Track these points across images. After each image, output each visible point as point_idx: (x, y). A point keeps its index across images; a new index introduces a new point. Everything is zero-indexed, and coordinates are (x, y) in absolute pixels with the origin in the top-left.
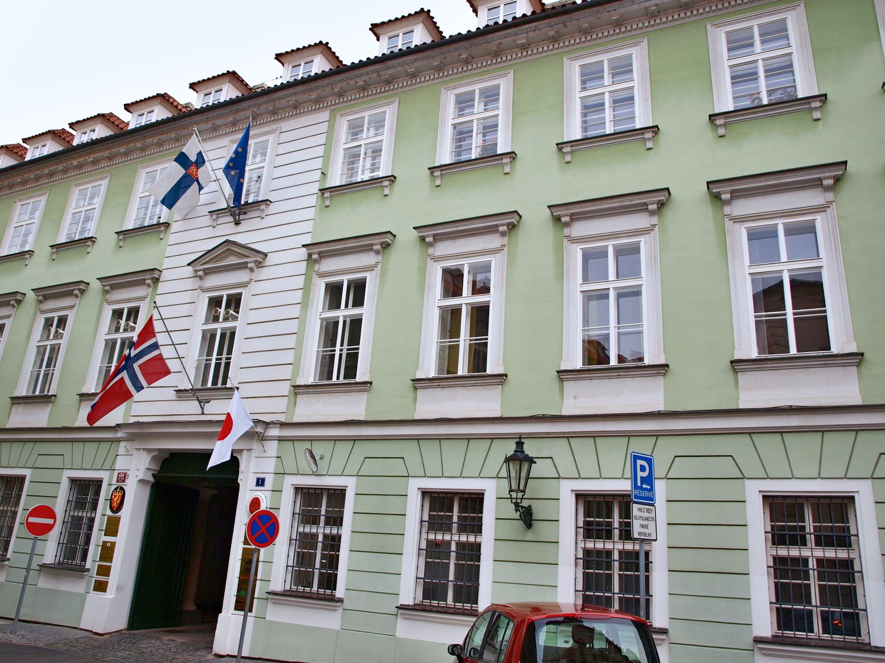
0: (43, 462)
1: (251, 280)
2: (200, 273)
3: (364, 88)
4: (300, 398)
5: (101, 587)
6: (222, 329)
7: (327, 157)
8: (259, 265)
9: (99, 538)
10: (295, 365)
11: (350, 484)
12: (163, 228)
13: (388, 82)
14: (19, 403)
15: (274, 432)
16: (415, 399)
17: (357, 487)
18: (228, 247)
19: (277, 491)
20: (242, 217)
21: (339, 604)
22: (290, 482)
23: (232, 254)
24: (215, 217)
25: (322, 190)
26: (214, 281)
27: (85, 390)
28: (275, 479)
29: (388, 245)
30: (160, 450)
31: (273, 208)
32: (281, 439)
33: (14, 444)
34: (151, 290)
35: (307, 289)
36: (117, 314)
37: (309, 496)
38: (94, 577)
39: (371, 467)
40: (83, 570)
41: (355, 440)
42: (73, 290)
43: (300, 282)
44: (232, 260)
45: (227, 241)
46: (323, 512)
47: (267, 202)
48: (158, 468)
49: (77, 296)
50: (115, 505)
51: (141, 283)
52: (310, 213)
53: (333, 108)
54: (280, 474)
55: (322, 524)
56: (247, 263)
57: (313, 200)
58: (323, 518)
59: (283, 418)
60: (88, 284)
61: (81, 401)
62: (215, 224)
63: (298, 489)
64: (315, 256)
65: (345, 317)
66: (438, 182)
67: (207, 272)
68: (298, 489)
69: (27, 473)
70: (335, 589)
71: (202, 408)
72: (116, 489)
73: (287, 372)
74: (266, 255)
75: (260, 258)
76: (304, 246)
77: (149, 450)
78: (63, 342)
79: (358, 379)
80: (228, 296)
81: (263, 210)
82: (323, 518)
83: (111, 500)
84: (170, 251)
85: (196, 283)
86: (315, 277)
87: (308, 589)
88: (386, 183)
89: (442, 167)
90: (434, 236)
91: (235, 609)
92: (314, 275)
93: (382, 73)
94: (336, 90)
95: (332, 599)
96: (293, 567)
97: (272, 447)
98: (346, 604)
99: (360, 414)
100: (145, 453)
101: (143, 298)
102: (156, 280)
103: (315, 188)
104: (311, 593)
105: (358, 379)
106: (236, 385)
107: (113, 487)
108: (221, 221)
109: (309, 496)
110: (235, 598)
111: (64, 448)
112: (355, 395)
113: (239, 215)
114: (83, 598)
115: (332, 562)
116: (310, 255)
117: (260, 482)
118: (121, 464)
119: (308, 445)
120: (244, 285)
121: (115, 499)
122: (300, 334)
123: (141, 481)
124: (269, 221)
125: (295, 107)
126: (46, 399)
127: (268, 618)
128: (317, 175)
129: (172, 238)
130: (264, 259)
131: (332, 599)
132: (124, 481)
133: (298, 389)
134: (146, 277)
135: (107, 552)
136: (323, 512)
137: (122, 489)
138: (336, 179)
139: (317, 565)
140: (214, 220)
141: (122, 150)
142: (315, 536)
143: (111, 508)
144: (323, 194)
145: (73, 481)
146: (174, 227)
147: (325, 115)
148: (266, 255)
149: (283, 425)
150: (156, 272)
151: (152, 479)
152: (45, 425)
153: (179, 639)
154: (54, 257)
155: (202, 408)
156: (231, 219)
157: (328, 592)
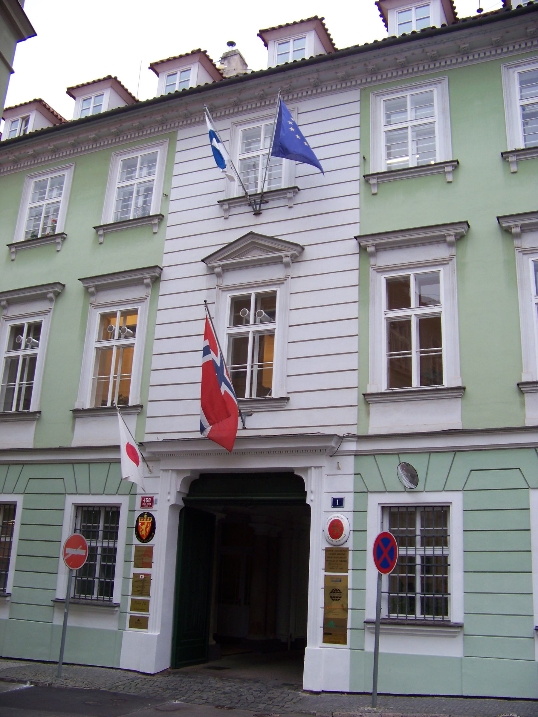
0: (34, 486)
1: (288, 276)
2: (219, 270)
3: (403, 66)
4: (373, 408)
5: (140, 623)
7: (365, 139)
8: (296, 259)
9: (127, 570)
10: (363, 370)
12: (156, 221)
13: (434, 59)
15: (352, 446)
16: (523, 404)
18: (252, 241)
19: (360, 512)
20: (263, 206)
21: (459, 630)
23: (255, 248)
24: (226, 207)
25: (367, 177)
27: (78, 406)
28: (355, 500)
30: (193, 471)
31: (302, 197)
32: (357, 454)
33: (12, 468)
34: (150, 290)
35: (363, 285)
36: (106, 319)
38: (129, 613)
39: (478, 480)
41: (455, 451)
42: (47, 293)
43: (354, 278)
44: (256, 255)
45: (251, 233)
46: (418, 532)
47: (295, 189)
49: (51, 300)
50: (143, 533)
51: (139, 282)
52: (355, 202)
53: (362, 87)
54: (361, 493)
55: (418, 545)
56: (281, 257)
57: (355, 187)
58: (418, 539)
59: (354, 431)
60: (64, 286)
61: (74, 418)
62: (227, 215)
63: (384, 508)
66: (514, 168)
67: (226, 269)
68: (384, 508)
72: (142, 515)
73: (352, 379)
75: (297, 253)
77: (178, 472)
78: (40, 352)
79: (446, 383)
80: (257, 295)
82: (418, 539)
83: (137, 527)
84: (169, 246)
85: (213, 281)
86: (372, 273)
88: (449, 169)
89: (515, 152)
90: (522, 226)
91: (324, 642)
92: (371, 270)
93: (427, 49)
94: (370, 67)
95: (447, 625)
97: (349, 464)
98: (467, 629)
100: (174, 475)
101: (141, 300)
102: (156, 280)
103: (356, 174)
105: (446, 383)
108: (234, 211)
110: (322, 630)
111: (65, 472)
112: (446, 402)
113: (260, 204)
114: (117, 637)
115: (442, 586)
117: (338, 503)
119: (394, 461)
121: (144, 527)
122: (362, 336)
125: (316, 86)
126: (27, 416)
128: (356, 160)
129: (170, 233)
132: (151, 506)
133: (369, 398)
134: (144, 276)
135: (142, 586)
136: (418, 532)
137: (150, 515)
138: (380, 164)
139: (418, 589)
140: (225, 210)
141: (92, 135)
142: (412, 559)
143: (139, 537)
145: (78, 507)
146: (170, 220)
147: (355, 95)
149: (360, 438)
150: (158, 270)
151: (182, 504)
152: (31, 446)
154: (13, 257)
157: (439, 617)
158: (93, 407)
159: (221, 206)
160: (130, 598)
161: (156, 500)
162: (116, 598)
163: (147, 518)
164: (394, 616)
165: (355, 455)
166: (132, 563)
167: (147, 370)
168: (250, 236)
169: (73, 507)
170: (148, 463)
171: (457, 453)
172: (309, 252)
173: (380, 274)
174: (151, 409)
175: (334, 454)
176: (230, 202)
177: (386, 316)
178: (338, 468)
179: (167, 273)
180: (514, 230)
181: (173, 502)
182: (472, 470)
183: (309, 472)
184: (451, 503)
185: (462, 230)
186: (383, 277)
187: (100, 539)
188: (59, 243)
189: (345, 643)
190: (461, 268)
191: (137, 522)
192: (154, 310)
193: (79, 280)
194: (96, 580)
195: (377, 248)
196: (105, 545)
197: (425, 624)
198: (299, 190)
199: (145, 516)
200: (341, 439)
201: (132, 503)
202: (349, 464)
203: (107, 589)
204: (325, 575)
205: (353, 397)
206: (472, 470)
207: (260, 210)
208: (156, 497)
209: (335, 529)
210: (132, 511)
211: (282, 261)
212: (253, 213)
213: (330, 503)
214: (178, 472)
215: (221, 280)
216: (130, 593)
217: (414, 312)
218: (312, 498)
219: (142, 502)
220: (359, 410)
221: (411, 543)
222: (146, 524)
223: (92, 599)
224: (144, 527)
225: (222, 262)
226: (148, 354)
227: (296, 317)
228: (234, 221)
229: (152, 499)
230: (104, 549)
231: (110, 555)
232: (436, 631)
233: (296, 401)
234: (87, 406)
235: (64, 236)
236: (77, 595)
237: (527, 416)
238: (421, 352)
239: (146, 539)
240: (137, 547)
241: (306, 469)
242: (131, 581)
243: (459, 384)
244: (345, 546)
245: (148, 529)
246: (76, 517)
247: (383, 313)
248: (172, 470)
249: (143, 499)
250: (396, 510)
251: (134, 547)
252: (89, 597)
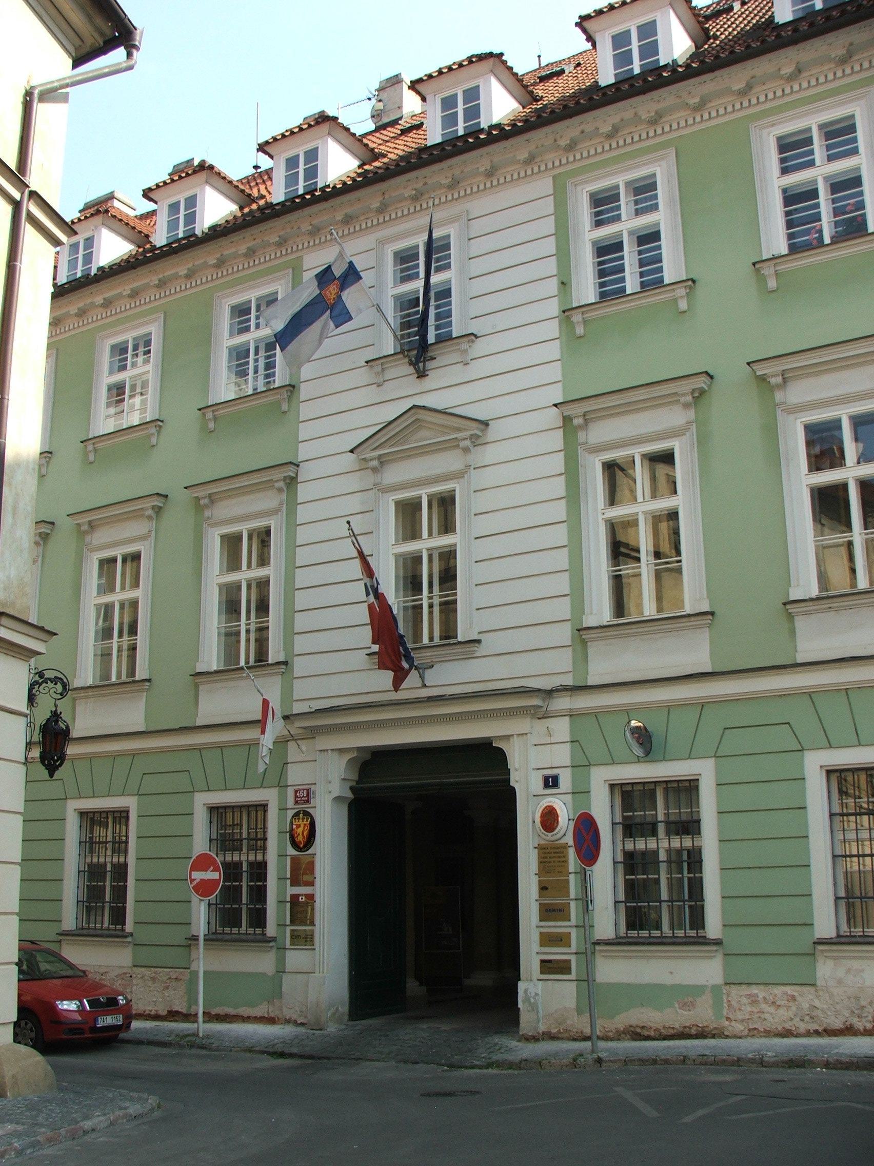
2: (375, 463)
6: (428, 549)
7: (563, 255)
8: (477, 441)
9: (281, 891)
10: (577, 594)
11: (705, 771)
14: (87, 697)
16: (793, 632)
17: (718, 771)
19: (581, 792)
22: (600, 779)
25: (567, 312)
26: (395, 474)
28: (573, 775)
29: (702, 392)
31: (480, 347)
37: (629, 795)
40: (266, 940)
43: (558, 463)
45: (414, 407)
46: (661, 817)
47: (472, 336)
48: (356, 777)
50: (300, 839)
52: (554, 350)
54: (581, 766)
57: (552, 329)
59: (569, 681)
64: (578, 421)
65: (645, 513)
69: (130, 803)
70: (703, 927)
71: (422, 677)
72: (296, 815)
74: (486, 424)
76: (555, 405)
81: (466, 351)
85: (369, 479)
87: (656, 933)
99: (701, 660)
100: (336, 755)
101: (276, 511)
102: (292, 482)
103: (553, 308)
104: (661, 937)
106: (475, 637)
107: (290, 813)
108: (389, 375)
109: (629, 795)
116: (567, 420)
117: (551, 782)
118: (296, 776)
120: (458, 475)
121: (300, 830)
123: (338, 799)
124: (478, 369)
128: (552, 286)
129: (305, 411)
131: (703, 941)
132: (308, 801)
136: (661, 817)
137: (307, 814)
140: (377, 374)
143: (295, 844)
144: (568, 318)
146: (305, 391)
147: (545, 185)
151: (349, 795)
153: (445, 1027)
156: (411, 370)
158: (222, 668)
159: (372, 367)
160: (288, 929)
161: (314, 793)
162: (271, 929)
163: (303, 819)
164: (634, 933)
166: (288, 882)
167: (290, 611)
168: (413, 411)
169: (205, 809)
170: (299, 742)
173: (594, 455)
174: (300, 666)
177: (604, 517)
179: (305, 473)
180: (773, 381)
181: (336, 793)
183: (511, 739)
185: (701, 382)
186: (597, 459)
187: (245, 850)
190: (703, 442)
191: (291, 823)
192: (292, 525)
193: (186, 488)
194: (244, 908)
196: (252, 858)
197: (674, 942)
199: (301, 815)
200: (549, 693)
201: (282, 798)
202: (561, 728)
203: (259, 919)
205: (564, 634)
207: (425, 370)
208: (312, 787)
209: (549, 819)
210: (283, 809)
211: (458, 445)
212: (416, 375)
213: (541, 783)
214: (341, 751)
215: (379, 475)
216: (288, 922)
217: (642, 506)
218: (517, 779)
219: (296, 797)
220: (574, 651)
221: (653, 831)
222: (302, 826)
223: (239, 934)
224: (300, 830)
225: (379, 449)
226: (290, 589)
227: (484, 525)
228: (391, 390)
229: (308, 791)
230: (251, 864)
231: (259, 870)
233: (491, 643)
234: (215, 668)
235: (161, 424)
236: (220, 930)
237: (798, 649)
238: (656, 565)
239: (305, 846)
240: (294, 859)
241: (507, 737)
242: (288, 905)
243: (706, 608)
244: (562, 841)
245: (305, 833)
246: (211, 822)
247: (600, 512)
248: (332, 750)
249: (296, 792)
250: (629, 788)
251: (289, 859)
252: (235, 930)
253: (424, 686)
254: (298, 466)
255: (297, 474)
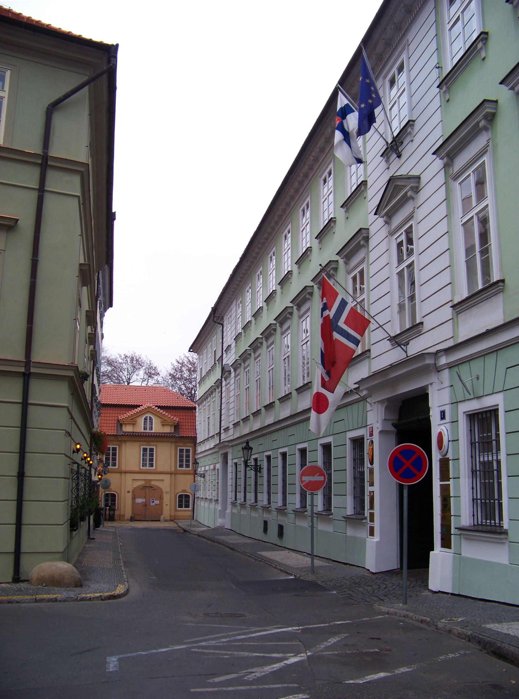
8: (417, 190)
15: (443, 361)
31: (418, 125)
32: (450, 366)
54: (455, 403)
71: (406, 352)
74: (418, 178)
96: (481, 500)
98: (511, 536)
127: (463, 554)
130: (419, 182)
148: (418, 178)
150: (363, 231)
151: (393, 429)
155: (406, 352)
165: (450, 368)
171: (498, 351)
172: (424, 179)
173: (456, 181)
175: (438, 370)
176: (386, 152)
178: (442, 383)
182: (507, 368)
184: (498, 405)
188: (332, 226)
189: (450, 548)
195: (451, 155)
198: (414, 121)
204: (441, 485)
205: (447, 312)
206: (507, 368)
207: (399, 153)
232: (494, 538)
253: (407, 356)
254: (368, 229)
255: (368, 233)
